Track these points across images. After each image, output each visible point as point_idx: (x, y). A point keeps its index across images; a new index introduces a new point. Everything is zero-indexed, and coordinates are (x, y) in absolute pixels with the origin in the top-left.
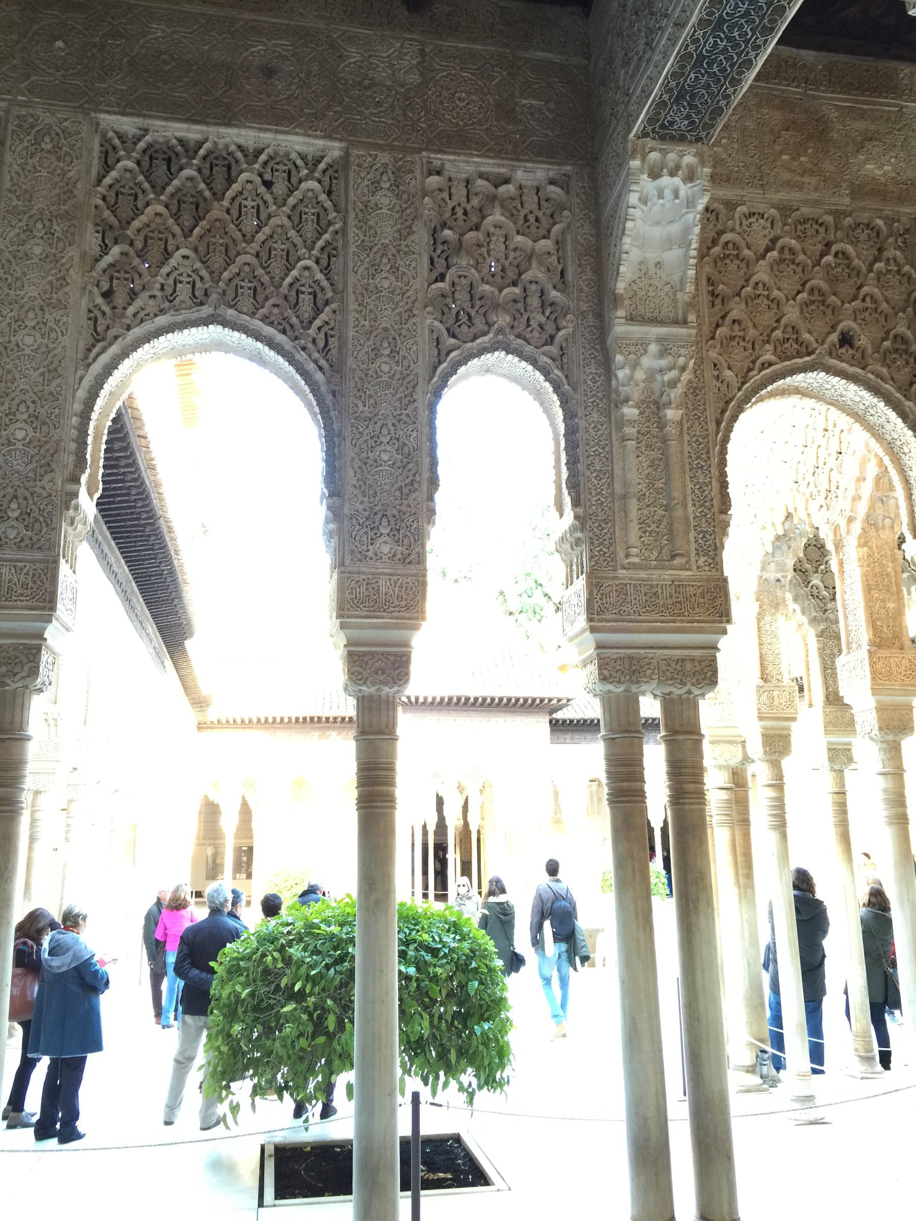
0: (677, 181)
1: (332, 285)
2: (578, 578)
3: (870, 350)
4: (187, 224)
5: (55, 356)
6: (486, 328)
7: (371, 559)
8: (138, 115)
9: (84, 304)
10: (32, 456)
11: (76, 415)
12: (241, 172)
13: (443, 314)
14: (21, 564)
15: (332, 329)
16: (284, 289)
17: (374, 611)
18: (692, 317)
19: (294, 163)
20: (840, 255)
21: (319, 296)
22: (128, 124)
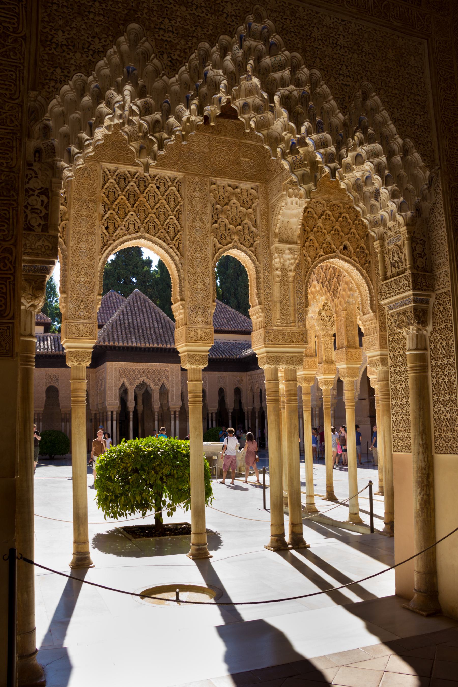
0: (297, 199)
3: (353, 251)
6: (230, 241)
8: (116, 163)
9: (100, 232)
12: (149, 184)
18: (299, 242)
22: (112, 167)
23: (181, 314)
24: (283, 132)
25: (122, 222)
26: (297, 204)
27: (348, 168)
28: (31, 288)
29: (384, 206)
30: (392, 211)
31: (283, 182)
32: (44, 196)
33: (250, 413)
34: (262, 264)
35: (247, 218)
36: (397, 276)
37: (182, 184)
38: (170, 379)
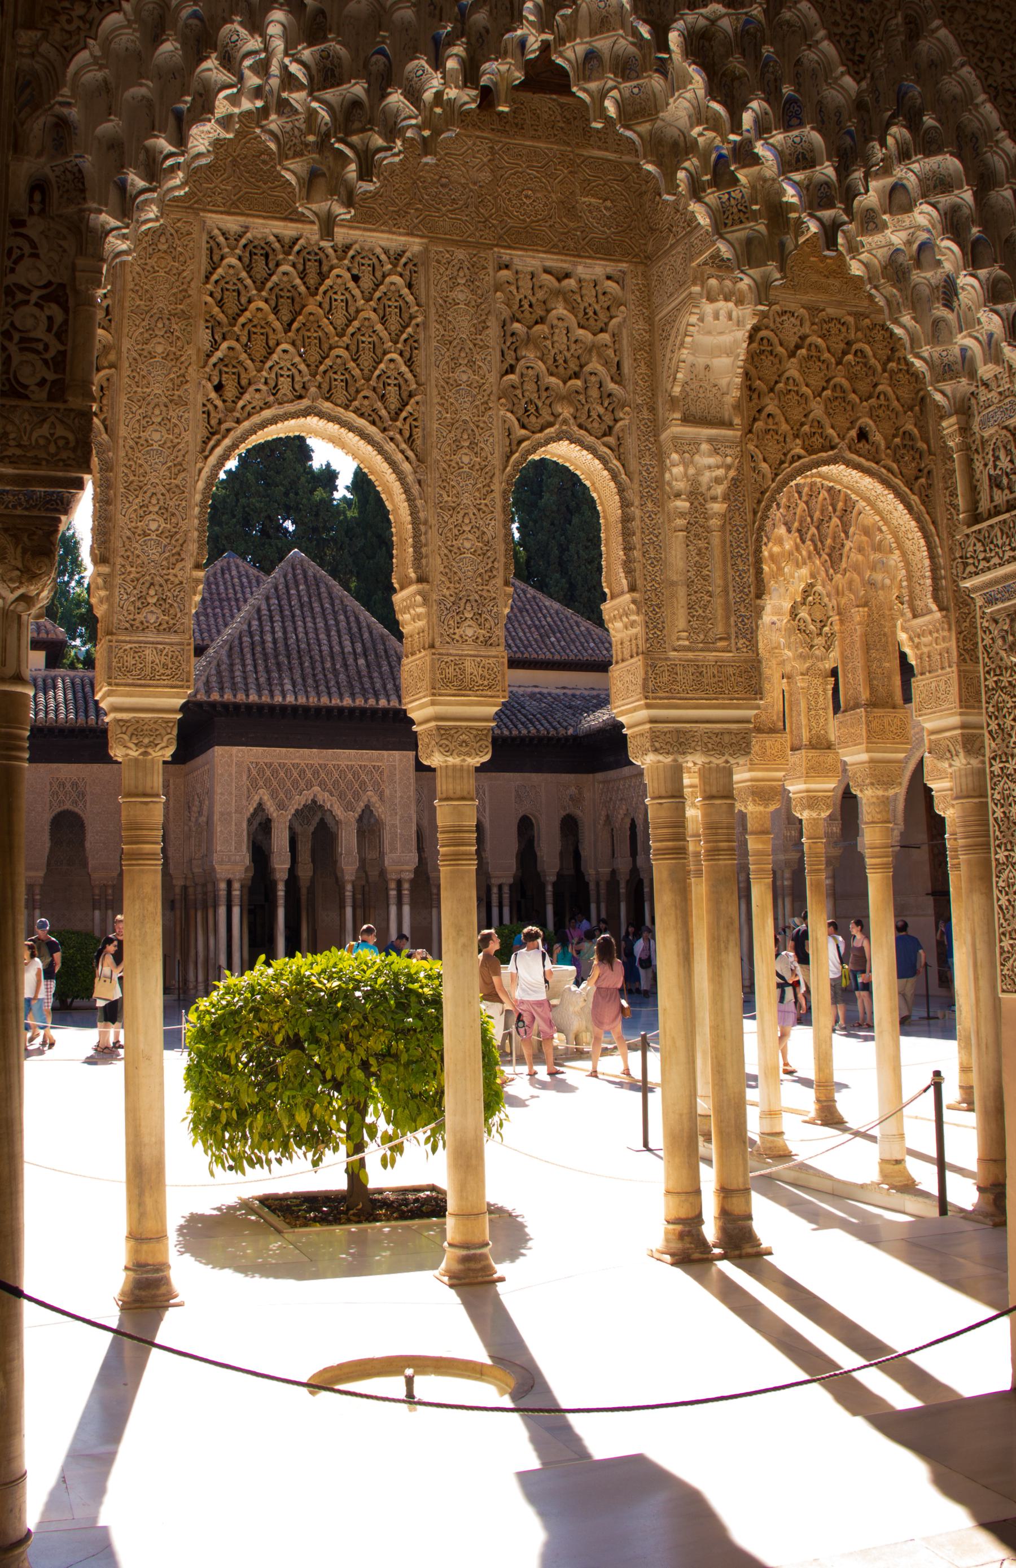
0: (731, 305)
4: (285, 318)
6: (551, 419)
8: (242, 214)
9: (200, 399)
12: (332, 268)
18: (737, 421)
21: (404, 387)
22: (232, 223)
23: (418, 617)
24: (692, 127)
25: (259, 371)
26: (730, 318)
27: (870, 222)
28: (19, 550)
29: (968, 323)
30: (991, 336)
31: (692, 260)
32: (54, 306)
33: (602, 884)
34: (636, 478)
36: (1008, 511)
37: (421, 269)
38: (387, 792)
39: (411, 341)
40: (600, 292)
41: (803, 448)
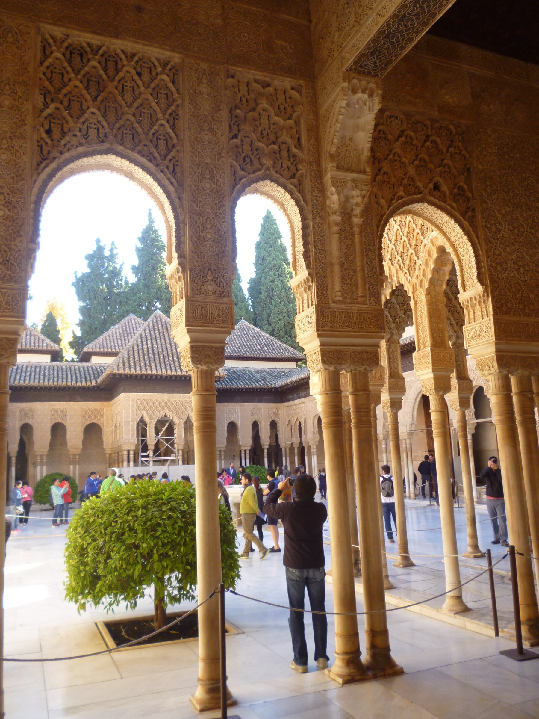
0: (366, 96)
1: (176, 135)
2: (308, 307)
3: (448, 193)
4: (93, 94)
5: (20, 167)
6: (260, 167)
7: (203, 293)
8: (64, 26)
9: (35, 136)
10: (9, 227)
11: (33, 203)
12: (124, 66)
13: (237, 157)
14: (4, 291)
15: (177, 161)
16: (150, 136)
17: (205, 323)
19: (153, 63)
20: (433, 142)
21: (169, 141)
22: (58, 32)
25: (76, 123)
31: (342, 65)
33: (288, 449)
35: (285, 134)
39: (174, 115)
40: (288, 96)
41: (404, 191)
